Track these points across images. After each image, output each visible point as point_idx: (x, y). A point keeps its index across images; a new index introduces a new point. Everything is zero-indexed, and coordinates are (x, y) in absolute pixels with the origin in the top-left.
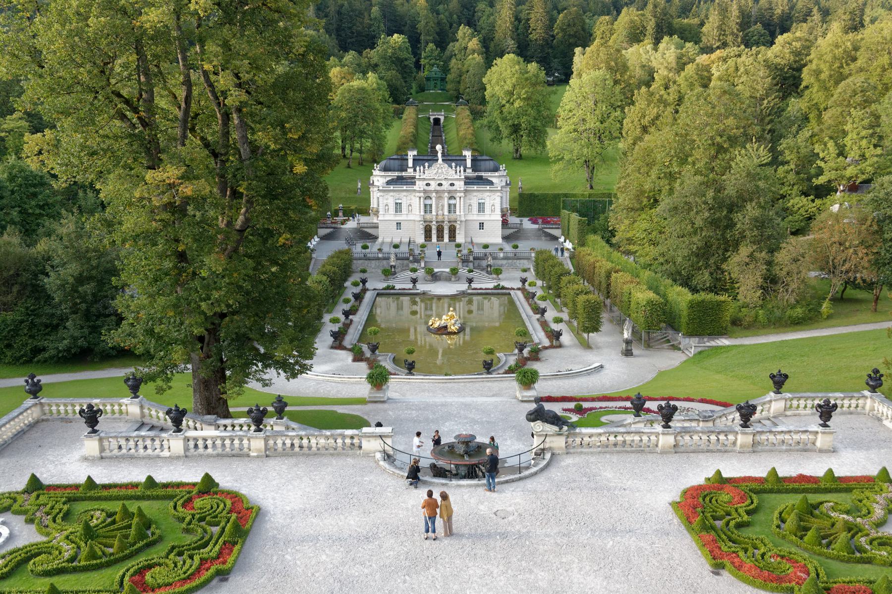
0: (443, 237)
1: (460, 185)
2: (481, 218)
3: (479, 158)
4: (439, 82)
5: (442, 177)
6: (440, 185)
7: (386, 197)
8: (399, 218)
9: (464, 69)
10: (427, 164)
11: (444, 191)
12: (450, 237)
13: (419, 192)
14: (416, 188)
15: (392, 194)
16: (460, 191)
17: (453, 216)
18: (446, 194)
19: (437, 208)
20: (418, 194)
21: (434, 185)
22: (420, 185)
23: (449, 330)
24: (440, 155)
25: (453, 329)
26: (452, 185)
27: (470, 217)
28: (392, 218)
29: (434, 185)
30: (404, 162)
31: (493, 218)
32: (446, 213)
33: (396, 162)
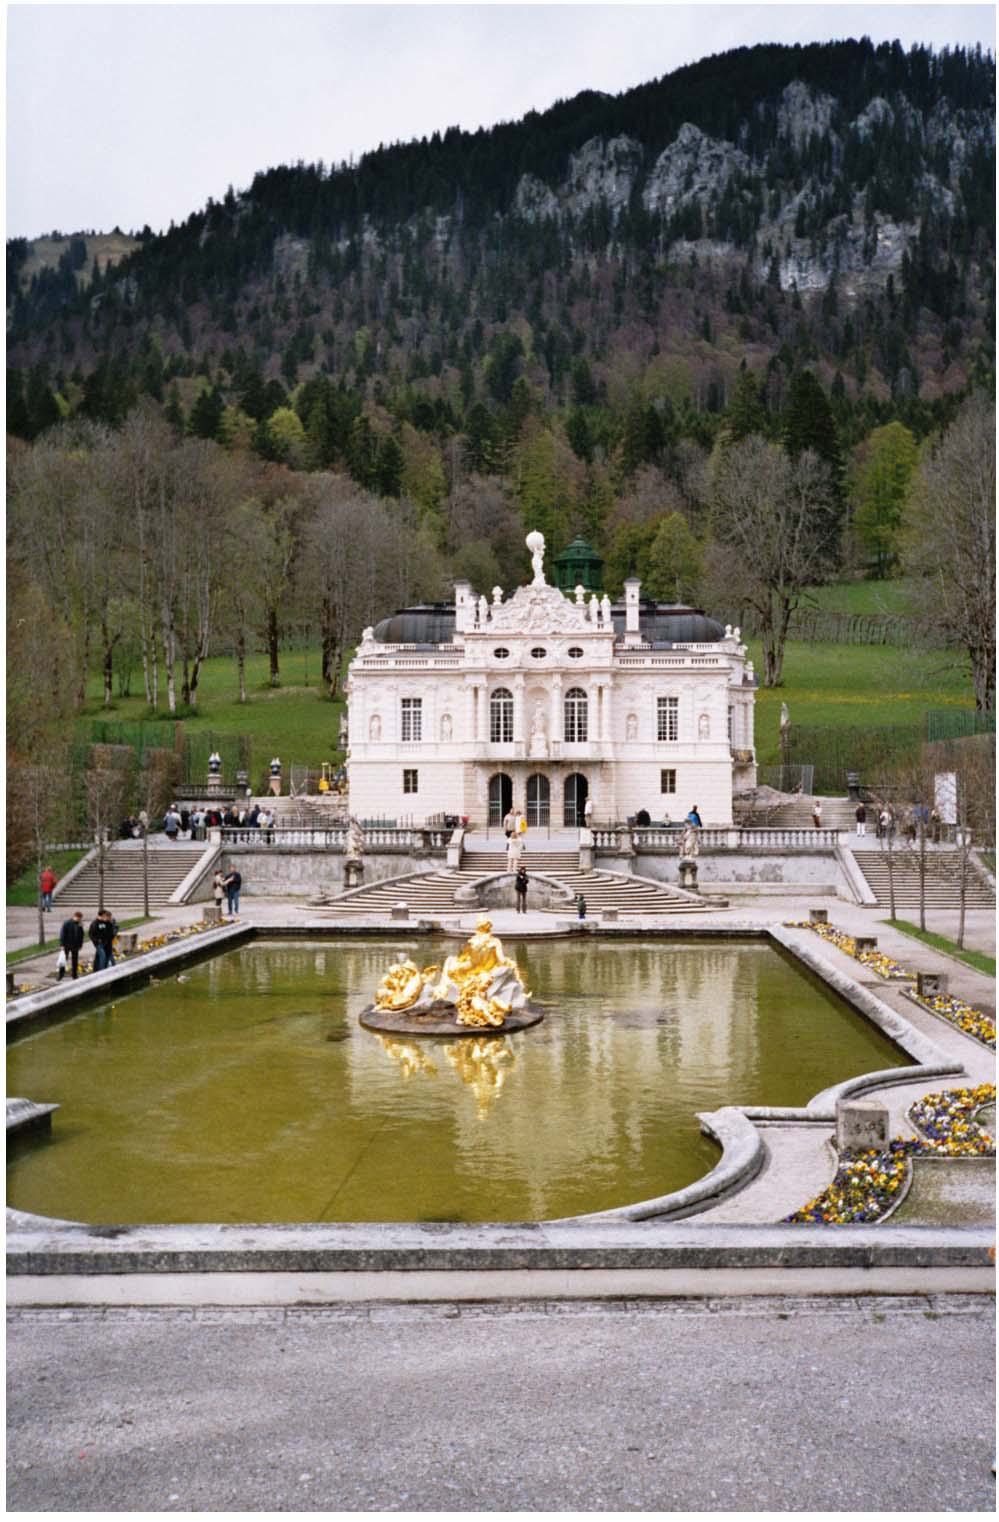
0: (546, 813)
1: (598, 654)
2: (667, 755)
3: (661, 608)
4: (586, 572)
5: (547, 628)
6: (538, 653)
7: (374, 691)
8: (411, 755)
9: (643, 536)
10: (497, 591)
11: (549, 674)
12: (567, 812)
13: (476, 673)
14: (464, 664)
15: (391, 681)
16: (600, 671)
17: (577, 751)
18: (557, 679)
19: (530, 723)
20: (471, 681)
21: (519, 652)
22: (477, 655)
23: (463, 1017)
24: (537, 563)
25: (486, 1009)
26: (576, 652)
27: (628, 753)
28: (388, 754)
29: (519, 652)
30: (447, 618)
31: (703, 754)
32: (557, 730)
33: (424, 618)
